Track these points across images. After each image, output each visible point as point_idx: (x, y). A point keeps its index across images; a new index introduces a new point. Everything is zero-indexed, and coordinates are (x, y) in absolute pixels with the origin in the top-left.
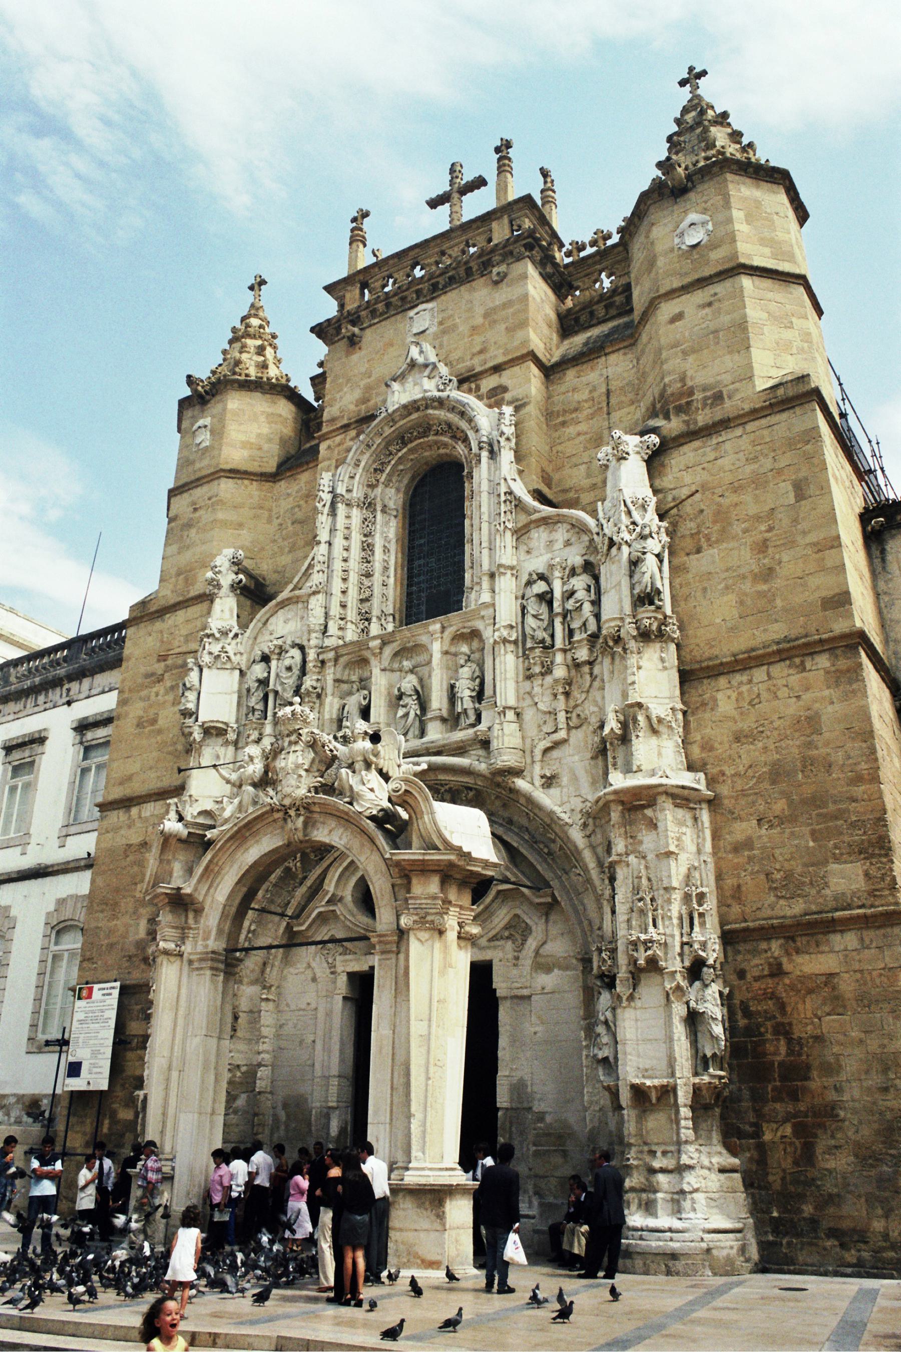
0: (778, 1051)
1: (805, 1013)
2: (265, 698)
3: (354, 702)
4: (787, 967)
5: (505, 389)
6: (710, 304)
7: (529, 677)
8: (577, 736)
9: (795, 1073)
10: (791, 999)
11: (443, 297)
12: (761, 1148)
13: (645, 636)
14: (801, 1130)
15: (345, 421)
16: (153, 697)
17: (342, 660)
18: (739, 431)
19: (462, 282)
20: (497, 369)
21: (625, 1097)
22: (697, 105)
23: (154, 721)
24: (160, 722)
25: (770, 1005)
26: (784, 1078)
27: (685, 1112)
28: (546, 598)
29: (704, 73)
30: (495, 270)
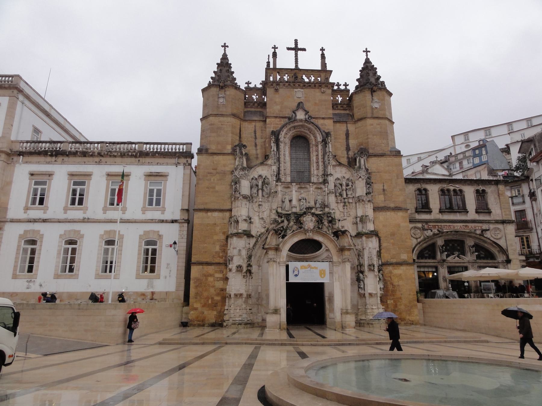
0: (390, 287)
1: (396, 281)
2: (258, 191)
3: (287, 198)
4: (393, 272)
5: (326, 125)
6: (379, 125)
7: (338, 203)
8: (348, 218)
9: (393, 291)
10: (393, 278)
11: (305, 90)
12: (388, 304)
13: (369, 201)
14: (394, 301)
15: (275, 115)
16: (212, 180)
17: (282, 186)
18: (385, 159)
19: (312, 88)
20: (323, 118)
21: (367, 295)
22: (367, 61)
23: (214, 188)
24: (217, 189)
25: (389, 279)
26: (392, 292)
27: (379, 298)
28: (341, 185)
29: (370, 52)
30: (323, 89)
